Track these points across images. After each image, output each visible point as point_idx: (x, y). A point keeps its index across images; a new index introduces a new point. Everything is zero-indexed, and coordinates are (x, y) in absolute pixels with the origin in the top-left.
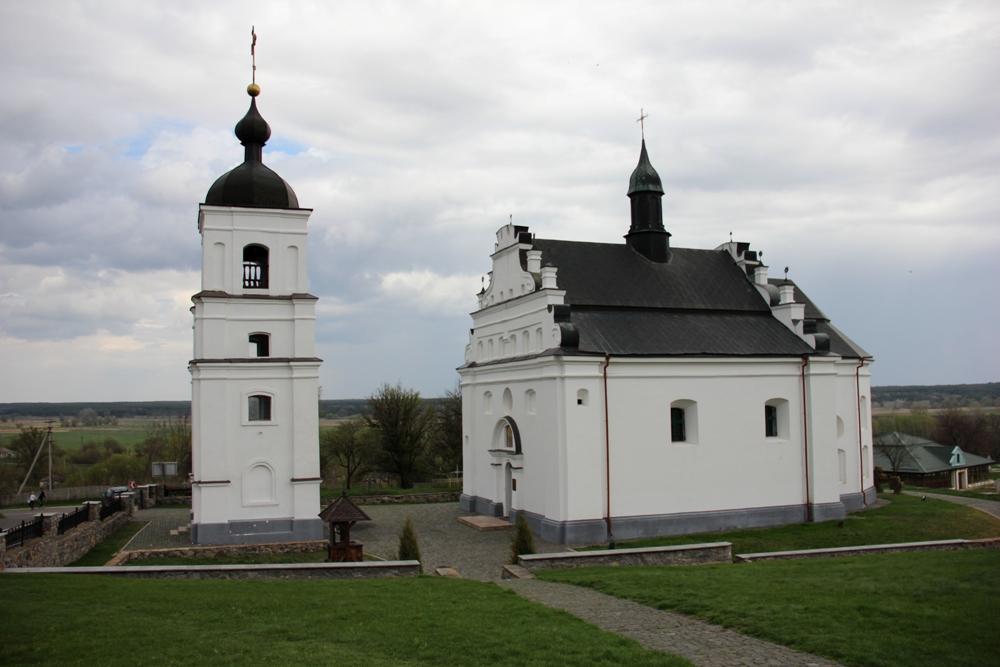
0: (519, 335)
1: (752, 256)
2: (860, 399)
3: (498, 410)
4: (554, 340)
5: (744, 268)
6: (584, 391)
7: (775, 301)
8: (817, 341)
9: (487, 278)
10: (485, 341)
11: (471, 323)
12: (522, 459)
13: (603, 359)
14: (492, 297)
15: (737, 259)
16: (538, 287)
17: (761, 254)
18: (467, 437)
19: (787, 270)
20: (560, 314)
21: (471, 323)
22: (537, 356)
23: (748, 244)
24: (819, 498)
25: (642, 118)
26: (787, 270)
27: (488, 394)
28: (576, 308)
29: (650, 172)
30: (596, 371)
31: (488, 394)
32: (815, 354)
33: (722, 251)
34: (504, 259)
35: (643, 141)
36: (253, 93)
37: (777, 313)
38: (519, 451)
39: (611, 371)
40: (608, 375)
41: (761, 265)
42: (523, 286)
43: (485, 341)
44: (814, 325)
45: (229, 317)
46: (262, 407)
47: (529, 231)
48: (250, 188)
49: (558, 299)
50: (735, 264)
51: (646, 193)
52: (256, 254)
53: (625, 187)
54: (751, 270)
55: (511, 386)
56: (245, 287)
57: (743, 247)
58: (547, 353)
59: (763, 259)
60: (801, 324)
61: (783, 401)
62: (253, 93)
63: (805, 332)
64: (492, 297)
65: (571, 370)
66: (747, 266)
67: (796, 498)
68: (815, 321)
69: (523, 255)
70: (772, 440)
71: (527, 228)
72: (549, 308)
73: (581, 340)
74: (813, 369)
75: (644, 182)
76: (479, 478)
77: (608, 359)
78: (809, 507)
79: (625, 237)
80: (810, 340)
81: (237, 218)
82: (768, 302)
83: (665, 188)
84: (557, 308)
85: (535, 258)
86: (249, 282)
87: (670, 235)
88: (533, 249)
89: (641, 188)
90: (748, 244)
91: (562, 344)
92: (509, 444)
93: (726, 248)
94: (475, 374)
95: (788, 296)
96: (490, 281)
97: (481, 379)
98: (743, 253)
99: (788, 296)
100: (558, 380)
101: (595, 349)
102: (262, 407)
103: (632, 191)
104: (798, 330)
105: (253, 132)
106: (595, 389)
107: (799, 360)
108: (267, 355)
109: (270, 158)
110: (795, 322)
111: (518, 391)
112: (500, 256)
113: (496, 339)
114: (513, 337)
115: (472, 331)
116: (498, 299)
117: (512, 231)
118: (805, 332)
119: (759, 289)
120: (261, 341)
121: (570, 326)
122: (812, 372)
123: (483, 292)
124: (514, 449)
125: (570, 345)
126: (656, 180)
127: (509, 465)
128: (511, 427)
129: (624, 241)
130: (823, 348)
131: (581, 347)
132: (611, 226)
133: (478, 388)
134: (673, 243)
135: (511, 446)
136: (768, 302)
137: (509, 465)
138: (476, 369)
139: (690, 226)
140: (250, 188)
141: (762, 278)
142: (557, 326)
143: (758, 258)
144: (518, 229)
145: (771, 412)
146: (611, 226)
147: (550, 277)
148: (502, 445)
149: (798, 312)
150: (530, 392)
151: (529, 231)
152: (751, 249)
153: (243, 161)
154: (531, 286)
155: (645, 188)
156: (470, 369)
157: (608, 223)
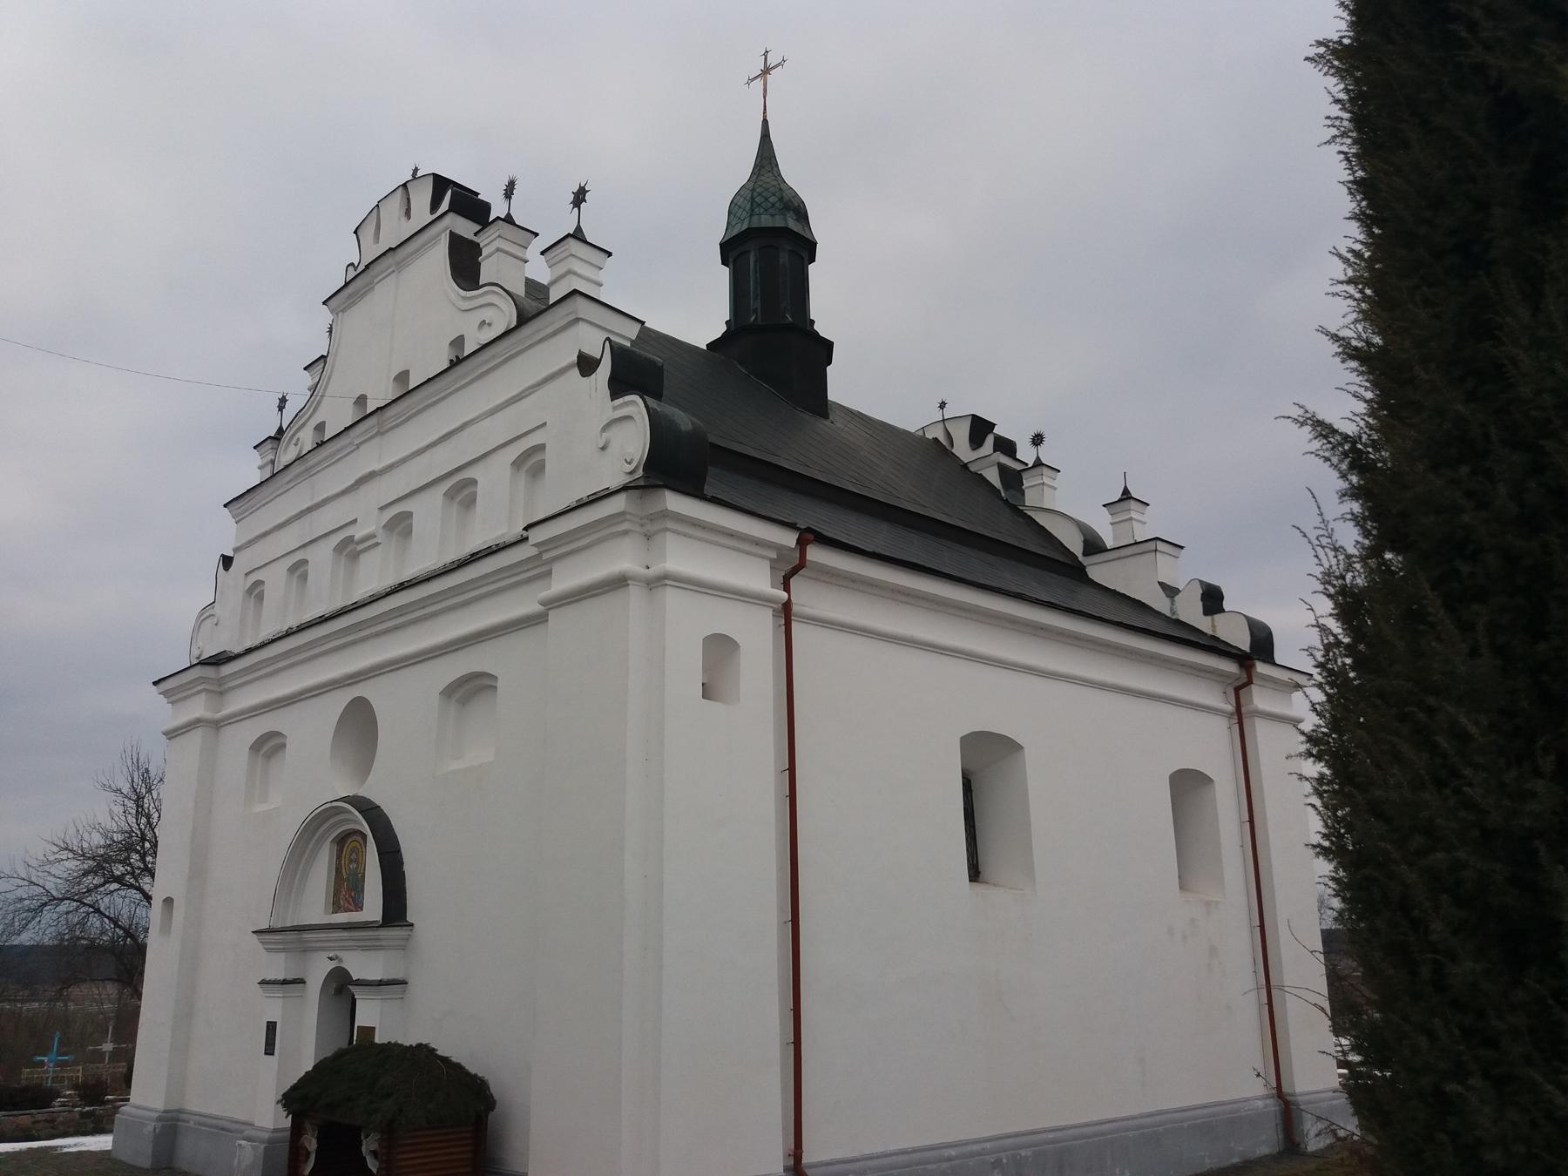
3: (314, 777)
6: (720, 649)
9: (308, 379)
11: (225, 533)
12: (404, 946)
13: (789, 539)
14: (320, 428)
17: (1038, 440)
18: (169, 901)
21: (225, 533)
25: (766, 71)
33: (923, 439)
34: (384, 295)
35: (765, 122)
37: (1099, 571)
38: (395, 910)
39: (806, 596)
40: (795, 608)
41: (1038, 463)
50: (965, 466)
51: (769, 244)
54: (1013, 479)
57: (980, 428)
59: (1046, 454)
65: (680, 557)
66: (1003, 469)
67: (1246, 1086)
74: (1260, 699)
78: (1288, 1110)
89: (766, 221)
92: (346, 891)
93: (937, 433)
94: (220, 691)
96: (314, 389)
98: (990, 440)
100: (635, 593)
107: (1230, 667)
112: (370, 288)
113: (322, 558)
114: (400, 525)
115: (227, 562)
117: (422, 197)
119: (1041, 519)
124: (373, 908)
126: (802, 214)
127: (341, 987)
131: (708, 490)
133: (229, 732)
135: (359, 907)
137: (341, 987)
138: (227, 669)
143: (1026, 453)
148: (314, 906)
155: (779, 223)
156: (209, 672)
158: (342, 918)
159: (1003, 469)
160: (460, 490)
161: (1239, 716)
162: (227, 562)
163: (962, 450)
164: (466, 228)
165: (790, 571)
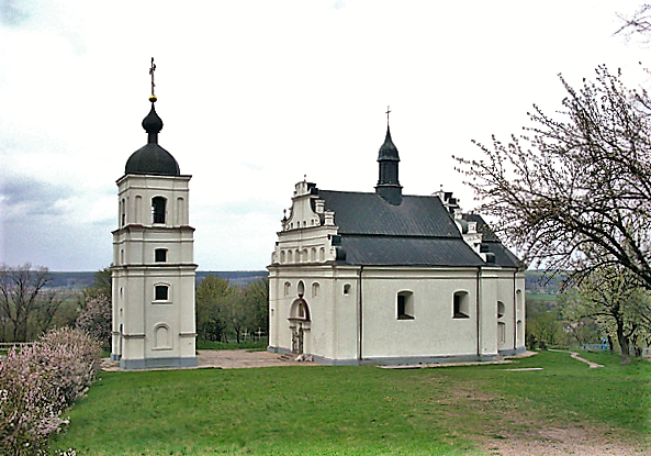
0: (309, 250)
1: (453, 201)
4: (332, 257)
7: (465, 232)
8: (487, 256)
9: (288, 212)
10: (286, 251)
15: (444, 203)
16: (322, 222)
22: (321, 265)
27: (288, 284)
29: (392, 148)
31: (288, 284)
36: (153, 100)
38: (308, 319)
41: (458, 207)
43: (286, 251)
44: (487, 247)
46: (162, 292)
48: (152, 162)
52: (159, 203)
53: (376, 156)
56: (155, 222)
57: (448, 195)
58: (327, 263)
62: (153, 100)
68: (490, 240)
69: (313, 201)
73: (347, 257)
75: (388, 155)
76: (280, 333)
77: (362, 266)
80: (483, 256)
85: (319, 209)
89: (386, 158)
91: (337, 258)
94: (278, 271)
97: (281, 274)
99: (472, 226)
102: (162, 292)
104: (477, 249)
105: (153, 125)
106: (354, 284)
109: (164, 140)
110: (476, 245)
111: (308, 284)
113: (294, 251)
114: (306, 251)
115: (277, 243)
116: (295, 227)
120: (161, 255)
123: (285, 220)
125: (341, 258)
126: (395, 152)
128: (302, 304)
129: (374, 191)
130: (490, 261)
132: (365, 179)
134: (404, 192)
139: (415, 181)
140: (152, 162)
144: (311, 185)
145: (459, 298)
146: (365, 179)
147: (329, 222)
150: (316, 285)
152: (453, 197)
153: (145, 142)
160: (314, 250)
161: (478, 278)
162: (277, 243)
163: (442, 199)
165: (360, 272)
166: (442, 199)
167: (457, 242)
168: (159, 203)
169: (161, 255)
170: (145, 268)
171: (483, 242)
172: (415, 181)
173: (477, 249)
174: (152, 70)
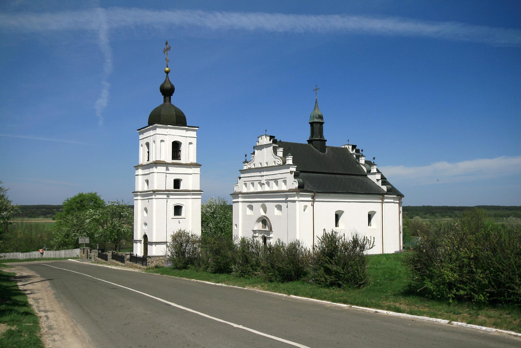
1: (358, 151)
2: (400, 212)
5: (355, 156)
6: (306, 207)
7: (369, 171)
17: (362, 151)
19: (374, 158)
20: (296, 176)
23: (356, 146)
24: (386, 252)
25: (316, 89)
26: (374, 158)
28: (301, 172)
30: (310, 199)
32: (386, 194)
42: (275, 162)
45: (167, 172)
46: (178, 210)
47: (275, 138)
49: (294, 169)
52: (176, 146)
54: (358, 157)
55: (266, 204)
56: (173, 159)
58: (290, 191)
59: (364, 153)
60: (380, 181)
61: (374, 213)
63: (382, 185)
64: (254, 165)
70: (369, 227)
71: (274, 137)
72: (291, 172)
75: (317, 118)
79: (308, 141)
80: (385, 188)
81: (168, 130)
82: (366, 171)
83: (325, 120)
84: (295, 172)
86: (173, 158)
87: (326, 141)
88: (280, 147)
89: (316, 120)
90: (356, 146)
91: (299, 187)
95: (374, 170)
101: (309, 190)
102: (178, 210)
103: (311, 121)
104: (379, 183)
107: (381, 196)
108: (179, 188)
109: (175, 100)
110: (378, 180)
117: (268, 138)
118: (382, 185)
120: (177, 183)
121: (301, 180)
122: (385, 200)
125: (301, 188)
128: (264, 221)
129: (307, 143)
134: (327, 144)
136: (366, 171)
141: (362, 161)
142: (296, 180)
143: (361, 152)
145: (370, 217)
147: (290, 161)
149: (379, 176)
151: (275, 138)
153: (162, 102)
154: (281, 162)
157: (302, 136)
158: (264, 229)
159: (356, 156)
163: (350, 150)
164: (274, 145)
166: (350, 150)
167: (363, 178)
168: (176, 146)
169: (177, 183)
170: (167, 193)
171: (381, 179)
172: (333, 138)
173: (379, 183)
174: (169, 49)
